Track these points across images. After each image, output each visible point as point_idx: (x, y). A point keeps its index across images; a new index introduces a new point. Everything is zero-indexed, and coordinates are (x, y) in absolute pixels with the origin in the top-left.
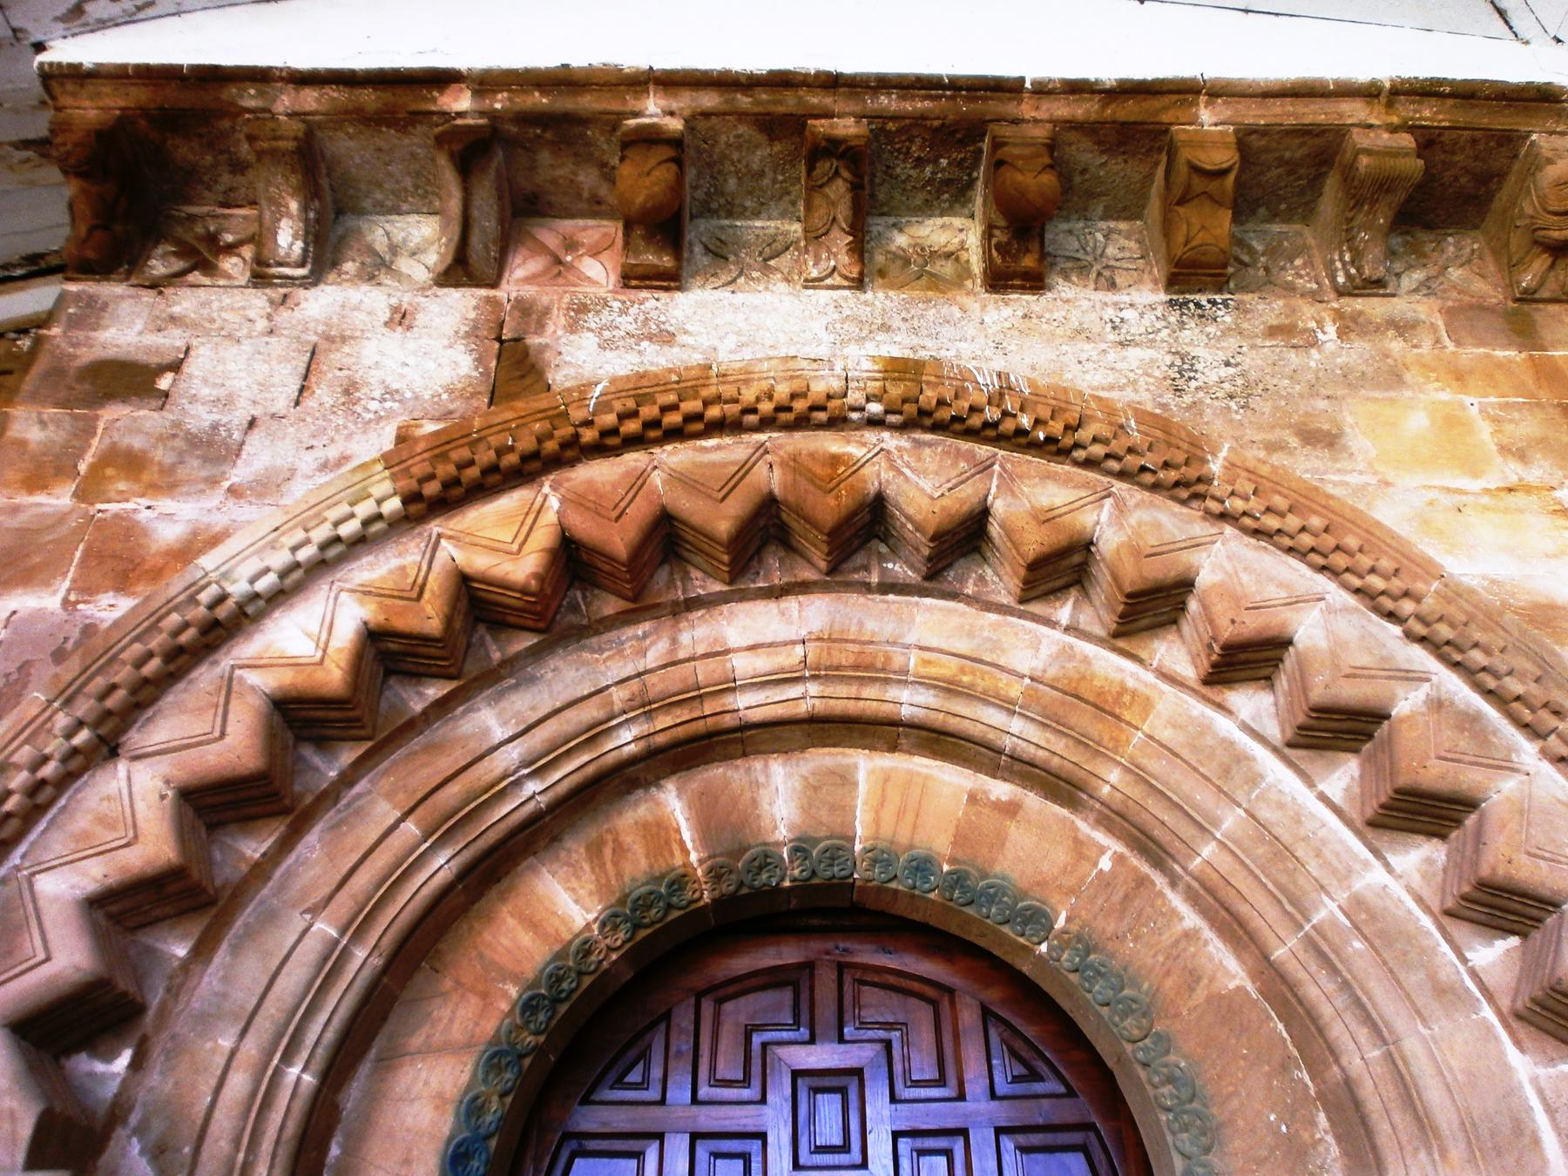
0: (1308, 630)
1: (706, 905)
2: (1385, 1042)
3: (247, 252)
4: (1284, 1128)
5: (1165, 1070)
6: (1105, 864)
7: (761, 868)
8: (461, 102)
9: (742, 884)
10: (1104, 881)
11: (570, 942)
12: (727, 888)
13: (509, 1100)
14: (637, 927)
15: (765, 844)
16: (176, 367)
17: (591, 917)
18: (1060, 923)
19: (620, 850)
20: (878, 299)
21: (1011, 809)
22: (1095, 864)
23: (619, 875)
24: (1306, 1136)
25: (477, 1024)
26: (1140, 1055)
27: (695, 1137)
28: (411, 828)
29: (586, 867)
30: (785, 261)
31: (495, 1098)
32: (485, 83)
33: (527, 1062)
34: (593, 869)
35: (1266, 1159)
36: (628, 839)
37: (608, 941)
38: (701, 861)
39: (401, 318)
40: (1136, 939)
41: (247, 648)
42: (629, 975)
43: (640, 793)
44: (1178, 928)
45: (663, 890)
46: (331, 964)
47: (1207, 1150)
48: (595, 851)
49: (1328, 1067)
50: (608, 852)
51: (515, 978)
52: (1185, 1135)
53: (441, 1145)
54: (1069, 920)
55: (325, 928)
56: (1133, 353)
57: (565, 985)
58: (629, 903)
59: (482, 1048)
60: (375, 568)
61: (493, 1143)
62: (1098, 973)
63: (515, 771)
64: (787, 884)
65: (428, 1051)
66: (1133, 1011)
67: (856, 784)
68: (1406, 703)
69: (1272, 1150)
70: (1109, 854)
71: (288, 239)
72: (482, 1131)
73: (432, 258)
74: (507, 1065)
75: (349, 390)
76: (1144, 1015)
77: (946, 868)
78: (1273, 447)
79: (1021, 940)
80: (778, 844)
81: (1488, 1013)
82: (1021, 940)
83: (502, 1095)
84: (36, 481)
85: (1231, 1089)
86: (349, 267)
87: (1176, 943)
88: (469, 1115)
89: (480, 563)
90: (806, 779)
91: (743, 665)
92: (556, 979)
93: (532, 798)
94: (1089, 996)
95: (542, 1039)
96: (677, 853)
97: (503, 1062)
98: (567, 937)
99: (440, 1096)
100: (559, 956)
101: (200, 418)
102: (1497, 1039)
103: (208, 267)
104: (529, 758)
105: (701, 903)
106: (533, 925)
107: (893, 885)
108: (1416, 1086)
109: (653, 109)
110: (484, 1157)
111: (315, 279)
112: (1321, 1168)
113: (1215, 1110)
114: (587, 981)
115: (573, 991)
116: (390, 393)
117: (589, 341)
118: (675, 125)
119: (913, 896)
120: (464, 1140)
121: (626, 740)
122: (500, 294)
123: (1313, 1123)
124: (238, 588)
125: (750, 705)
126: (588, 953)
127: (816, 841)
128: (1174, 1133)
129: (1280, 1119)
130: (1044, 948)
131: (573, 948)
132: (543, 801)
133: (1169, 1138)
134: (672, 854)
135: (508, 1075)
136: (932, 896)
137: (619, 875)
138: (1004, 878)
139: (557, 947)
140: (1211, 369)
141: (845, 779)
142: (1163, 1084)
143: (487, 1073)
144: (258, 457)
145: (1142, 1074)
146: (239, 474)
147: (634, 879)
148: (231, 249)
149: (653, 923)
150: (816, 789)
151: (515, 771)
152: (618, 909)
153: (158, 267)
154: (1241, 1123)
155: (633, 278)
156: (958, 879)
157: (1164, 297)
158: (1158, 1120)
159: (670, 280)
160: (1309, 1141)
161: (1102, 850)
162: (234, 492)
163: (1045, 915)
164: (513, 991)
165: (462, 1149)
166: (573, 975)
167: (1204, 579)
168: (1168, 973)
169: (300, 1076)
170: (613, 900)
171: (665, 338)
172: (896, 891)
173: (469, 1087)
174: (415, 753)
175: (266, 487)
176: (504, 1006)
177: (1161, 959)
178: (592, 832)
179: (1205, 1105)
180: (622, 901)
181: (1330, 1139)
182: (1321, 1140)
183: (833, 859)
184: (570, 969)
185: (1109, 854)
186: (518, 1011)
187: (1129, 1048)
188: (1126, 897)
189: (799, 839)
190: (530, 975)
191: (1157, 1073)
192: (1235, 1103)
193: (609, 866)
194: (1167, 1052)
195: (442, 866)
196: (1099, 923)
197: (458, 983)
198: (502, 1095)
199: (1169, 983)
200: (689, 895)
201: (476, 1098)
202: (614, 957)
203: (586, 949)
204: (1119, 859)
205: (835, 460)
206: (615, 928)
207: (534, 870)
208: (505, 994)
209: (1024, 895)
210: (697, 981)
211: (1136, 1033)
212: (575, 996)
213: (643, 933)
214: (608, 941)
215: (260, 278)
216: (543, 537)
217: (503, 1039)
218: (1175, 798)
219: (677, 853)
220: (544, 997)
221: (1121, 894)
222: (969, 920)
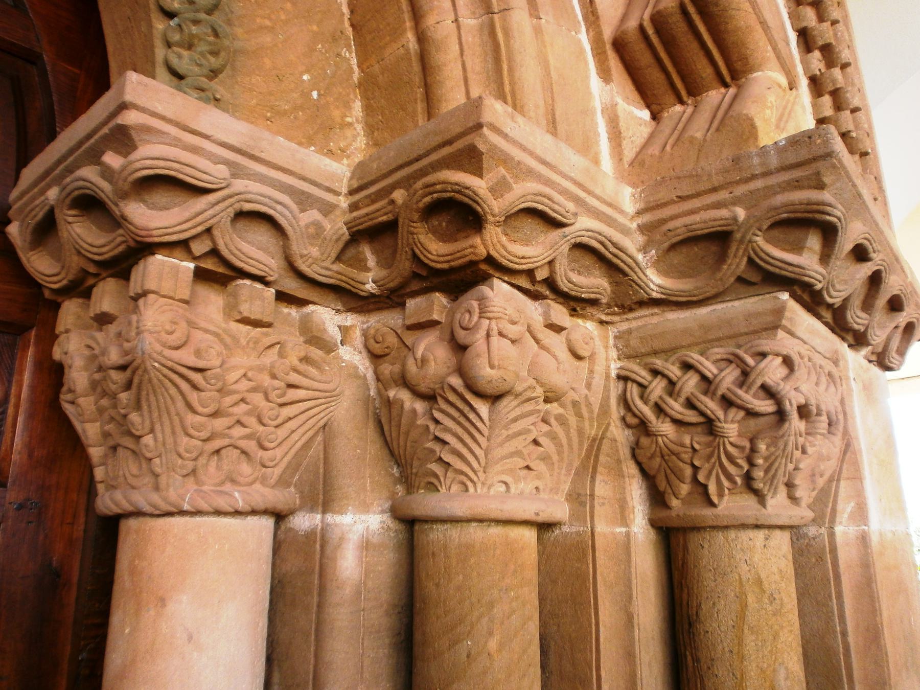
2: (489, 11)
4: (315, 94)
24: (336, 114)
35: (285, 113)
47: (214, 73)
49: (397, 33)
52: (185, 53)
69: (296, 109)
81: (584, 37)
85: (268, 23)
102: (586, 63)
108: (510, 60)
112: (343, 151)
113: (239, 31)
123: (347, 106)
128: (169, 45)
129: (314, 86)
133: (160, 52)
154: (268, 63)
158: (150, 26)
160: (338, 120)
179: (229, 23)
181: (359, 127)
182: (350, 124)
192: (267, 39)
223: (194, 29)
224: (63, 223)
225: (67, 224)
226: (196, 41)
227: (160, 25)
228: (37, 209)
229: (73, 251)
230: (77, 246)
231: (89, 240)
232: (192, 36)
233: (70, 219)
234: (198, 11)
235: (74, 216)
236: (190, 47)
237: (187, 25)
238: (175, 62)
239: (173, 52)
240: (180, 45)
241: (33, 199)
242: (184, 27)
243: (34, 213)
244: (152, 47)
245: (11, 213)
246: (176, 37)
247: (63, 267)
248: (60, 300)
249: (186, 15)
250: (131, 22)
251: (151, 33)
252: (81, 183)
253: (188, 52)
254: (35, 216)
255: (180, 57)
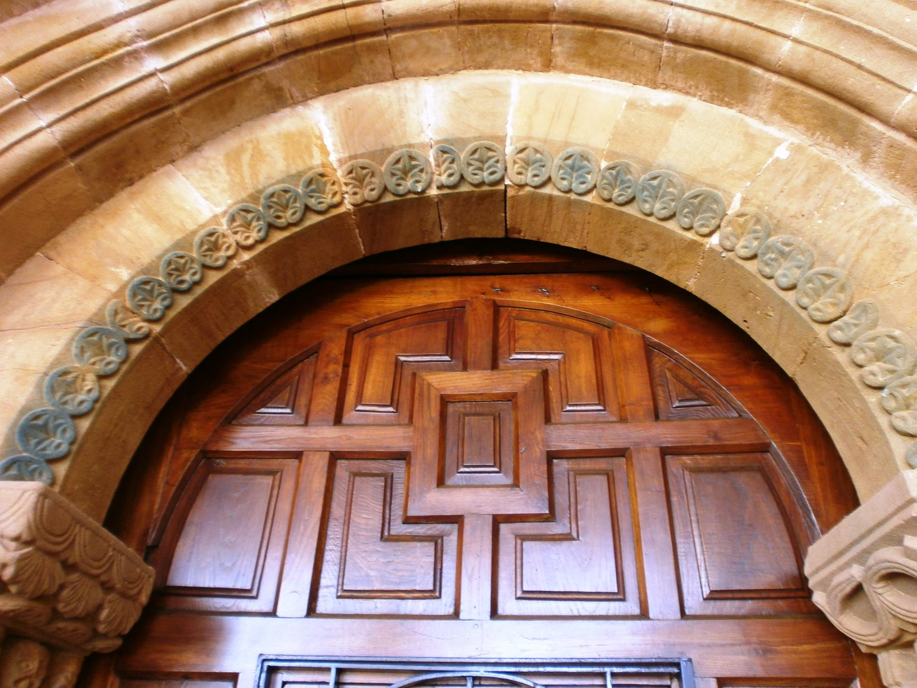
1: (347, 214)
5: (873, 344)
6: (782, 153)
7: (406, 172)
9: (385, 189)
10: (781, 168)
11: (194, 233)
12: (368, 194)
13: (110, 384)
14: (271, 227)
15: (410, 146)
17: (219, 210)
18: (734, 207)
19: (258, 155)
21: (675, 112)
22: (771, 153)
23: (255, 174)
25: (80, 303)
26: (839, 335)
29: (222, 170)
31: (90, 382)
33: (137, 349)
34: (229, 173)
36: (267, 147)
37: (238, 237)
38: (341, 162)
40: (825, 217)
42: (274, 297)
43: (287, 111)
44: (873, 207)
45: (300, 191)
48: (233, 159)
50: (246, 158)
51: (129, 263)
52: (905, 413)
53: (12, 415)
54: (745, 201)
57: (187, 277)
58: (262, 201)
59: (80, 324)
61: (85, 424)
62: (782, 254)
63: (132, 42)
64: (433, 192)
65: (26, 327)
66: (826, 288)
67: (508, 96)
70: (785, 145)
72: (71, 408)
74: (111, 345)
76: (842, 288)
77: (604, 164)
79: (690, 235)
80: (423, 146)
82: (690, 235)
83: (101, 377)
87: (874, 219)
88: (52, 389)
90: (456, 94)
92: (175, 267)
93: (152, 75)
94: (770, 283)
95: (157, 328)
96: (316, 152)
97: (105, 342)
98: (191, 227)
99: (24, 369)
100: (183, 244)
104: (148, 28)
105: (342, 210)
106: (158, 219)
107: (547, 190)
110: (69, 435)
114: (213, 278)
115: (197, 283)
119: (569, 203)
120: (45, 412)
126: (215, 247)
127: (463, 142)
128: (889, 413)
130: (715, 240)
131: (197, 239)
132: (168, 80)
133: (883, 420)
134: (311, 156)
135: (114, 358)
136: (588, 198)
137: (255, 174)
138: (668, 168)
139: (179, 236)
141: (498, 93)
142: (870, 361)
143: (82, 350)
145: (841, 356)
147: (268, 177)
149: (290, 225)
150: (465, 100)
151: (132, 42)
152: (251, 206)
156: (617, 173)
158: (863, 401)
161: (778, 142)
163: (716, 200)
164: (125, 274)
165: (40, 422)
166: (196, 267)
168: (867, 246)
170: (244, 195)
172: (551, 198)
173: (57, 361)
174: (28, 22)
176: (113, 287)
177: (857, 233)
178: (231, 142)
180: (254, 198)
183: (483, 162)
184: (193, 260)
185: (785, 145)
186: (127, 292)
187: (821, 331)
188: (808, 181)
189: (446, 141)
190: (146, 259)
191: (862, 350)
193: (246, 169)
194: (874, 325)
196: (781, 203)
197: (70, 268)
198: (101, 377)
199: (868, 255)
200: (328, 200)
201: (65, 373)
202: (246, 256)
203: (212, 242)
204: (797, 149)
206: (247, 225)
207: (169, 175)
208: (116, 277)
209: (693, 180)
210: (350, 319)
211: (832, 312)
212: (199, 291)
213: (278, 237)
214: (238, 237)
217: (108, 319)
218: (876, 31)
219: (316, 152)
220: (160, 284)
221: (803, 177)
222: (632, 226)
223: (905, 392)
224: (874, 594)
225: (879, 596)
226: (912, 401)
227: (872, 398)
228: (844, 585)
229: (890, 616)
230: (894, 613)
231: (906, 607)
232: (906, 399)
233: (880, 591)
234: (902, 376)
235: (882, 588)
236: (908, 407)
237: (898, 392)
238: (900, 424)
239: (897, 417)
240: (899, 409)
241: (833, 574)
242: (896, 394)
243: (840, 587)
244: (873, 418)
245: (811, 584)
246: (891, 404)
247: (880, 629)
248: (875, 652)
249: (894, 384)
250: (841, 401)
251: (868, 407)
252: (888, 564)
253: (908, 411)
254: (843, 590)
255: (904, 419)
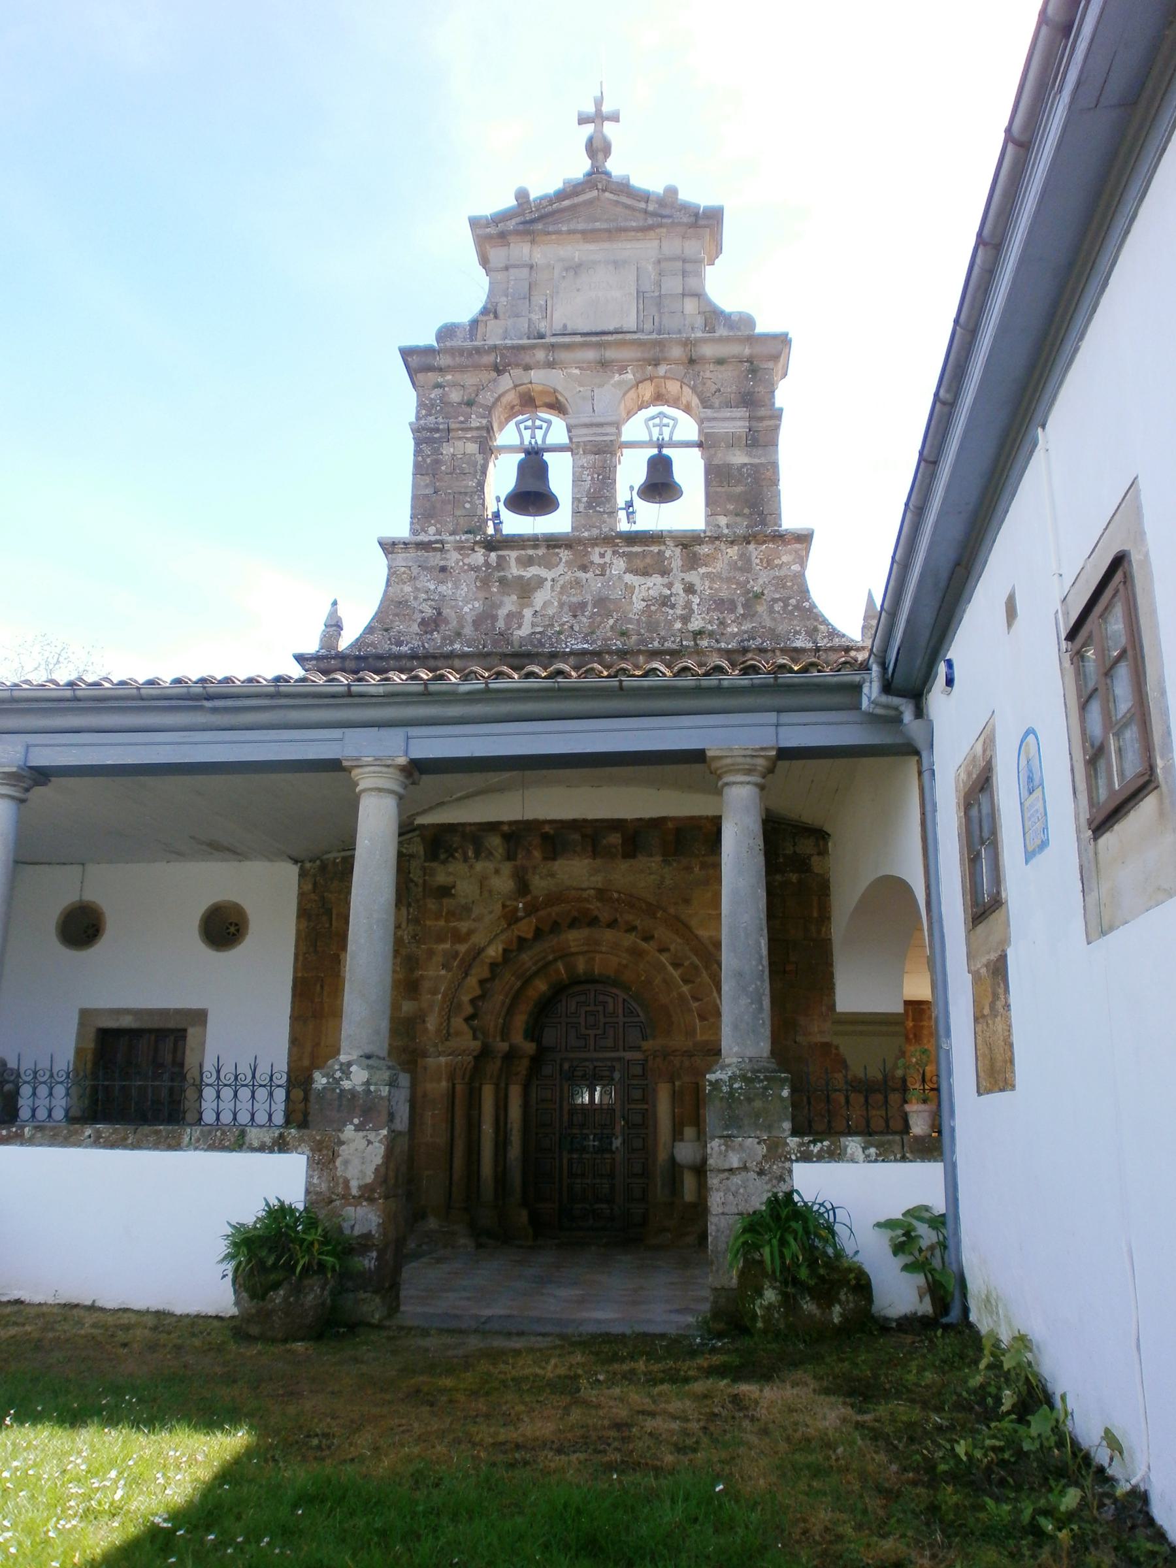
0: (672, 947)
3: (460, 851)
6: (643, 978)
8: (506, 828)
16: (454, 887)
20: (599, 861)
27: (567, 1024)
28: (513, 978)
30: (578, 849)
32: (510, 823)
39: (497, 872)
41: (483, 955)
46: (503, 1003)
55: (501, 997)
56: (653, 877)
60: (503, 937)
68: (687, 963)
71: (470, 853)
73: (500, 850)
75: (490, 891)
78: (675, 904)
84: (437, 918)
86: (483, 855)
89: (523, 935)
91: (572, 944)
101: (463, 901)
103: (452, 856)
109: (547, 828)
111: (477, 860)
116: (499, 893)
117: (537, 877)
118: (552, 832)
121: (551, 957)
122: (518, 863)
124: (482, 946)
125: (573, 950)
140: (668, 882)
144: (476, 911)
146: (473, 916)
148: (456, 850)
153: (442, 857)
155: (545, 859)
157: (661, 858)
159: (554, 859)
162: (474, 920)
167: (656, 936)
169: (501, 1021)
171: (552, 875)
175: (479, 919)
195: (519, 984)
205: (588, 909)
215: (466, 859)
216: (533, 928)
